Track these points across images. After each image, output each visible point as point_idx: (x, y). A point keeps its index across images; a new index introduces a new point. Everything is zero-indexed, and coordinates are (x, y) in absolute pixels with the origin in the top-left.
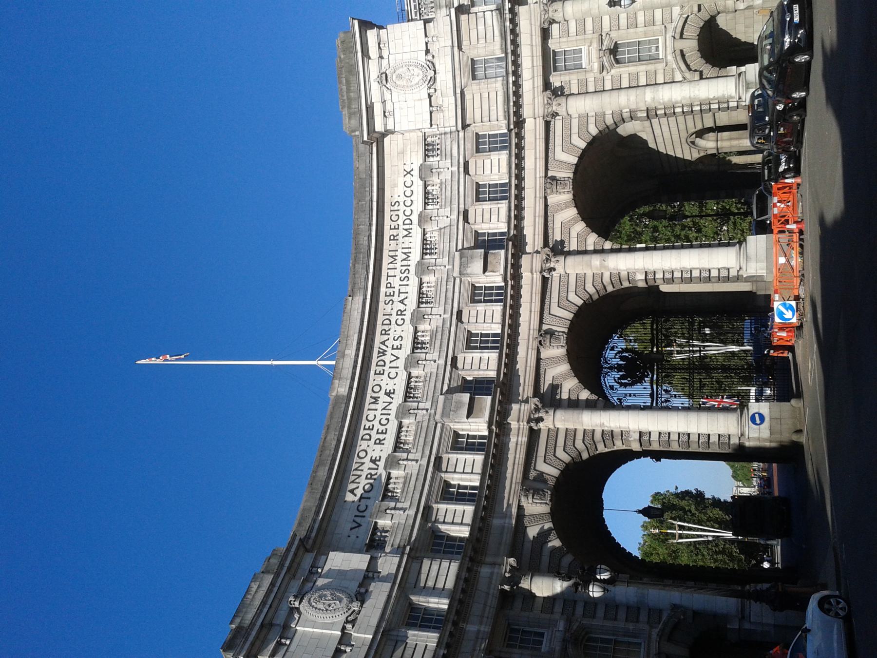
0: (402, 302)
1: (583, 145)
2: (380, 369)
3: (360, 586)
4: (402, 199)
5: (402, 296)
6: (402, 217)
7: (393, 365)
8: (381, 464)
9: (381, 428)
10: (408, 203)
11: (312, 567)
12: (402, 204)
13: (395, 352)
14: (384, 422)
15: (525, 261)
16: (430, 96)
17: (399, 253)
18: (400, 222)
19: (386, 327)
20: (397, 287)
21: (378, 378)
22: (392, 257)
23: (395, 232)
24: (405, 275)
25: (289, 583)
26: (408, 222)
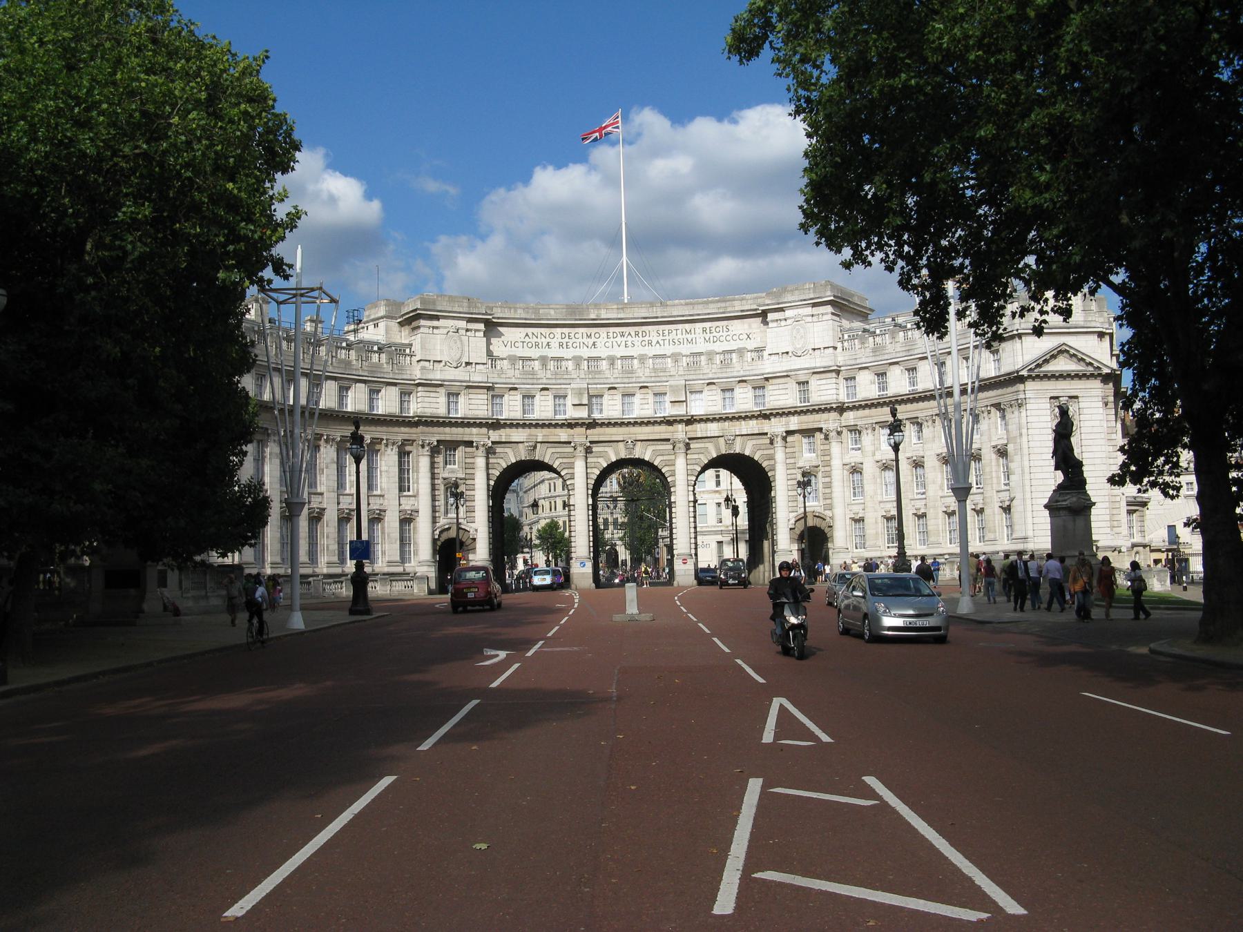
0: (658, 342)
1: (756, 458)
2: (611, 335)
3: (468, 364)
5: (661, 342)
6: (718, 335)
7: (614, 343)
9: (570, 344)
10: (728, 338)
12: (728, 333)
13: (623, 343)
15: (680, 427)
16: (787, 353)
17: (693, 336)
18: (715, 334)
19: (640, 335)
23: (708, 331)
26: (715, 339)
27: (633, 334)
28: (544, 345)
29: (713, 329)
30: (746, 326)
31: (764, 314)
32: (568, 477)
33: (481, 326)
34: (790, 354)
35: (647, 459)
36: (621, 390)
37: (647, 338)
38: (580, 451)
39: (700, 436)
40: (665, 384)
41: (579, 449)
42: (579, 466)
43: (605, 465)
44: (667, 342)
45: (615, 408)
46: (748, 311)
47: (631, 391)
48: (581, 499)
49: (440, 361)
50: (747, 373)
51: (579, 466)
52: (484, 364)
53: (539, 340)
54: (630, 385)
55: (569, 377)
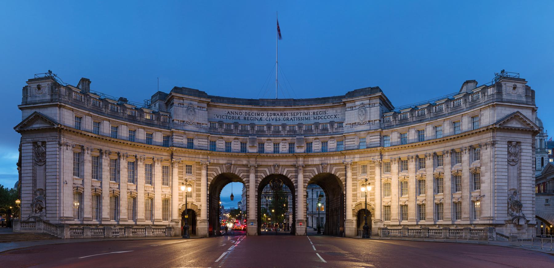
2: (269, 114)
4: (327, 115)
5: (293, 119)
7: (271, 119)
8: (238, 121)
9: (249, 118)
11: (202, 107)
12: (326, 115)
13: (275, 118)
14: (251, 119)
16: (356, 123)
17: (308, 116)
18: (319, 115)
19: (283, 115)
20: (296, 116)
21: (266, 115)
22: (307, 113)
23: (316, 114)
24: (300, 119)
25: (197, 102)
26: (319, 118)
27: (280, 114)
28: (237, 118)
29: (318, 113)
30: (334, 111)
31: (345, 104)
32: (246, 182)
33: (205, 105)
34: (357, 124)
35: (284, 174)
36: (273, 141)
37: (286, 117)
38: (252, 170)
39: (310, 163)
40: (295, 138)
41: (252, 168)
42: (252, 177)
43: (264, 177)
44: (296, 119)
45: (270, 149)
46: (336, 103)
47: (278, 142)
48: (253, 192)
49: (184, 121)
50: (335, 134)
51: (252, 177)
52: (206, 124)
53: (234, 115)
54: (278, 138)
55: (248, 133)
